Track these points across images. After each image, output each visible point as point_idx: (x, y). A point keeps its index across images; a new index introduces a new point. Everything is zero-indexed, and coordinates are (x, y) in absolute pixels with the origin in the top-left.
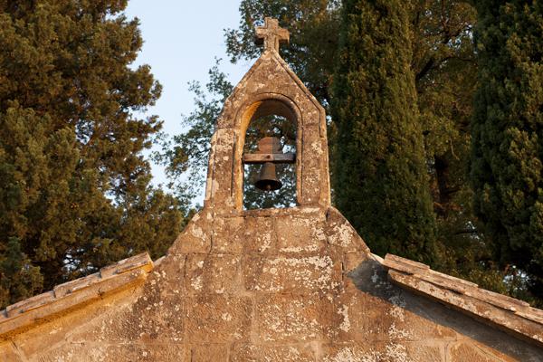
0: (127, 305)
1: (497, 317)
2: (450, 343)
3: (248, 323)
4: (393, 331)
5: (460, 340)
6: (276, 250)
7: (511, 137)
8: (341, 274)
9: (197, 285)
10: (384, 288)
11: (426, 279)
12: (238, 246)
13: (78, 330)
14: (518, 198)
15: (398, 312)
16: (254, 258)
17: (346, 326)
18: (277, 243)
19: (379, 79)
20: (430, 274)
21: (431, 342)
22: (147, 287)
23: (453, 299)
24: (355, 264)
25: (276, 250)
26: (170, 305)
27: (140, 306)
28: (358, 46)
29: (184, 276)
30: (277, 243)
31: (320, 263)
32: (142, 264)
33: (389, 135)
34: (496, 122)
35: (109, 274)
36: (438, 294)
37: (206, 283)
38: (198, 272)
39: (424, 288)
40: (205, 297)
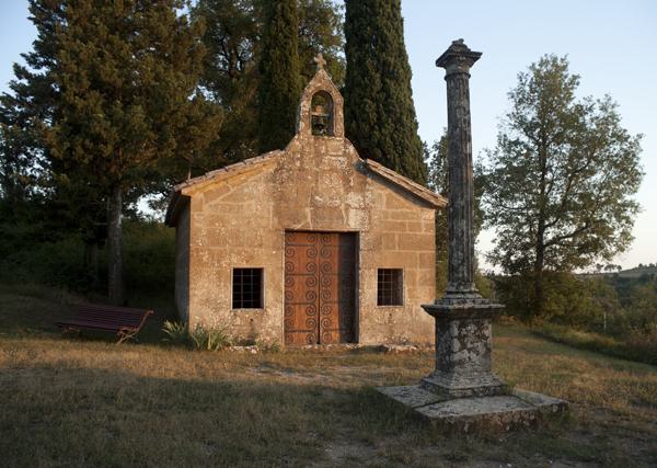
0: (271, 170)
1: (403, 185)
2: (386, 192)
3: (317, 180)
4: (367, 187)
5: (389, 191)
6: (327, 153)
7: (366, 103)
8: (350, 164)
9: (298, 164)
10: (366, 171)
11: (382, 170)
12: (313, 150)
13: (253, 178)
14: (367, 128)
15: (369, 180)
16: (318, 155)
17: (352, 184)
18: (327, 151)
19: (285, 55)
20: (383, 168)
21: (380, 191)
22: (279, 164)
23: (389, 177)
24: (355, 161)
25: (327, 153)
26: (288, 171)
27: (276, 170)
28: (276, 38)
29: (293, 160)
30: (327, 151)
31: (341, 159)
32: (279, 153)
33: (289, 84)
34: (360, 95)
35: (267, 158)
36: (385, 175)
37: (302, 163)
38: (298, 159)
39: (381, 173)
40: (301, 169)
